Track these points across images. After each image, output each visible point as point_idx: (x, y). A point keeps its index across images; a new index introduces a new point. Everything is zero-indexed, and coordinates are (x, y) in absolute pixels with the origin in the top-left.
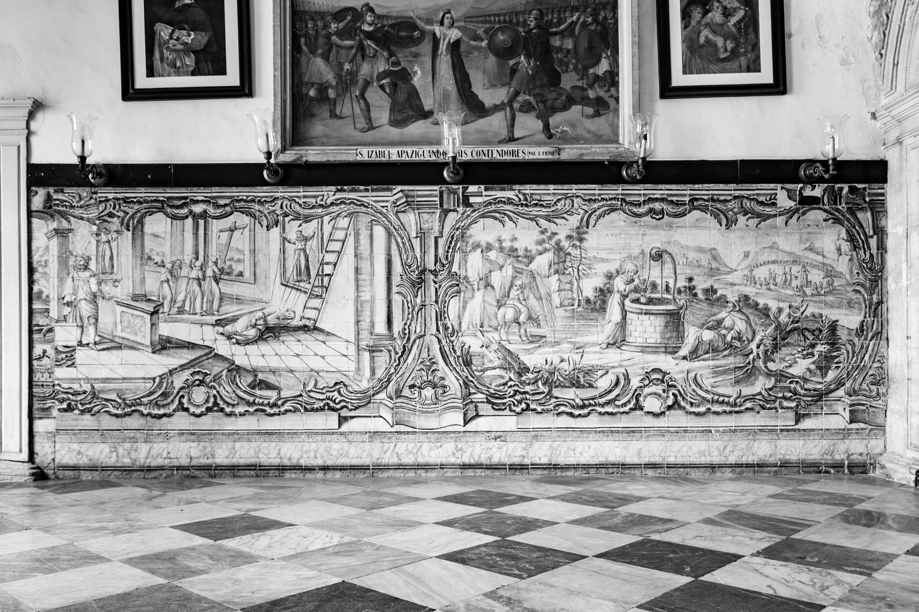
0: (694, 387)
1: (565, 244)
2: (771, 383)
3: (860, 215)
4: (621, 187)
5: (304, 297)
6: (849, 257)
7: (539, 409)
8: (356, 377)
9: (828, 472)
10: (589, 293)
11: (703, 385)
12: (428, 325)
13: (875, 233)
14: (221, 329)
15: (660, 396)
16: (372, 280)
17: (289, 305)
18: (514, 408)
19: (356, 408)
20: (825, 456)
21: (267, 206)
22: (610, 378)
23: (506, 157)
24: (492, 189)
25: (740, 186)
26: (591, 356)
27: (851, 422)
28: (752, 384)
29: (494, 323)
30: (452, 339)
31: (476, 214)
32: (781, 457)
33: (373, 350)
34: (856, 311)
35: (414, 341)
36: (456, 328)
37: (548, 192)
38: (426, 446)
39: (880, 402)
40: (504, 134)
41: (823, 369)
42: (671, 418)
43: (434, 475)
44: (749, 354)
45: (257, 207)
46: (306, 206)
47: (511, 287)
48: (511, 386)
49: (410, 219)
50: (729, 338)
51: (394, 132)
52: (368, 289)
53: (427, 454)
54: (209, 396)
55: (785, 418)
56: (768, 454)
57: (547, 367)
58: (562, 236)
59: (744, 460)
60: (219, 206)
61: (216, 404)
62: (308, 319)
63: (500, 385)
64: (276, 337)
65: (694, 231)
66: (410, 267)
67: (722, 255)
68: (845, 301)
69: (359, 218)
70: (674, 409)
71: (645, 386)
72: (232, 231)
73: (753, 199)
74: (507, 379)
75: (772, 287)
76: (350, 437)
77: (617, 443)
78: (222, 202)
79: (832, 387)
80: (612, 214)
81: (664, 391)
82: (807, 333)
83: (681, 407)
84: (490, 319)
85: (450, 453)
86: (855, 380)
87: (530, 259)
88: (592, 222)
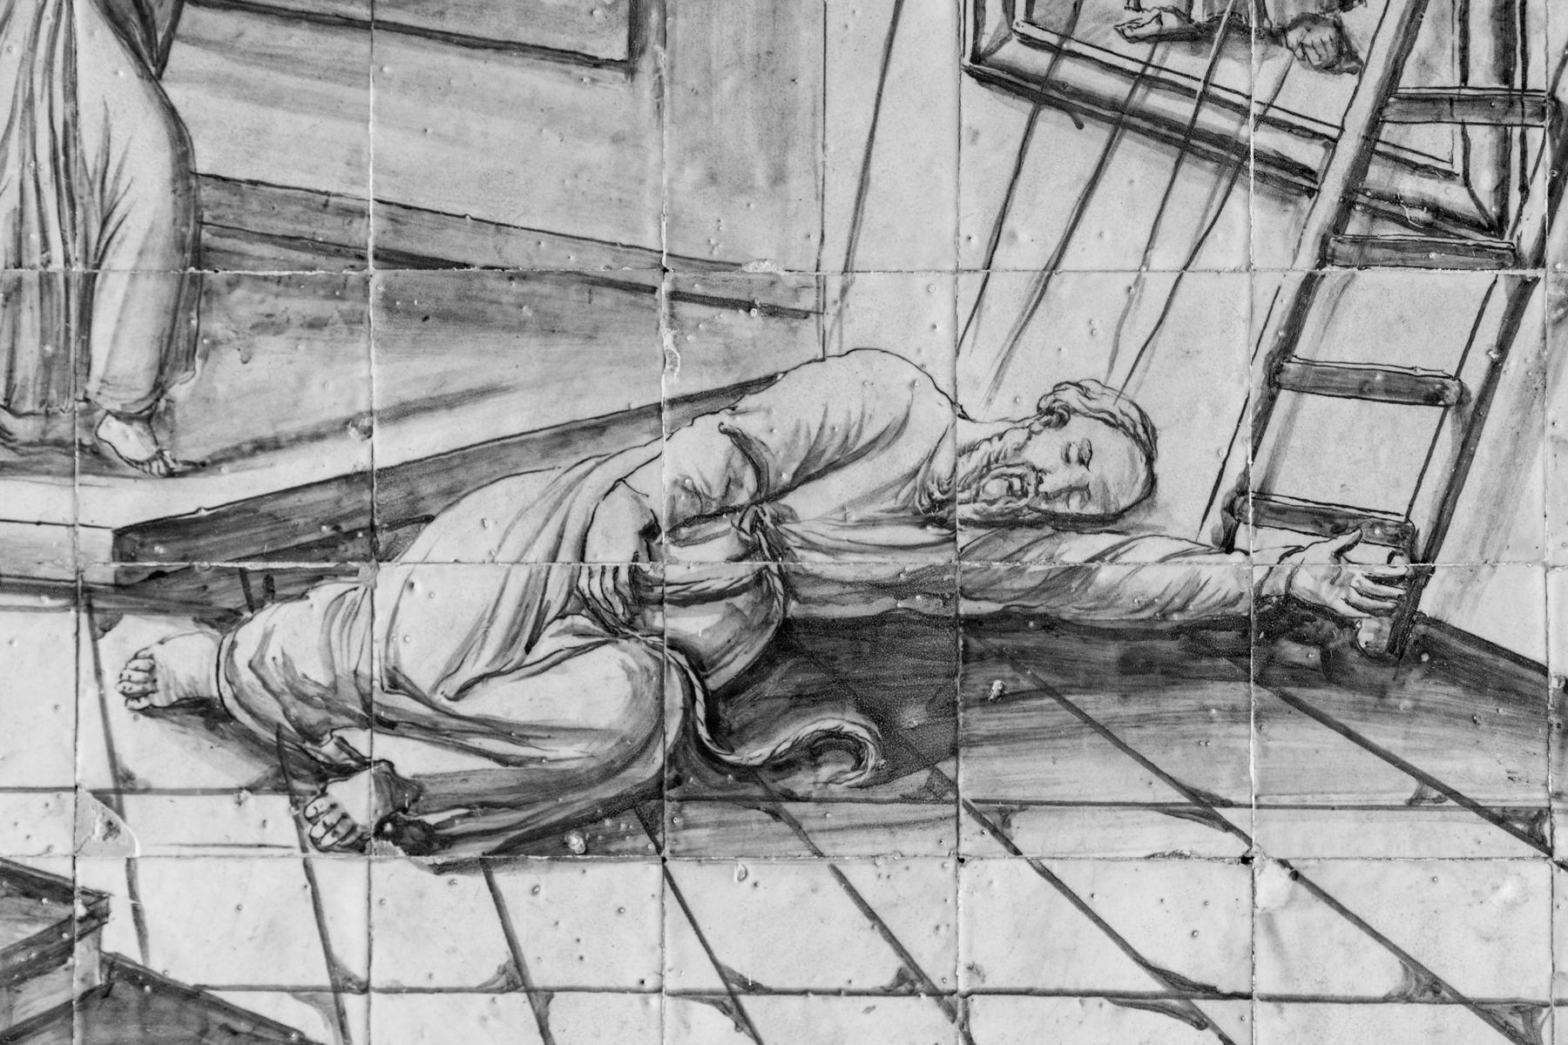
5: (1261, 241)
14: (187, 655)
17: (1071, 346)
62: (1326, 519)
64: (900, 754)
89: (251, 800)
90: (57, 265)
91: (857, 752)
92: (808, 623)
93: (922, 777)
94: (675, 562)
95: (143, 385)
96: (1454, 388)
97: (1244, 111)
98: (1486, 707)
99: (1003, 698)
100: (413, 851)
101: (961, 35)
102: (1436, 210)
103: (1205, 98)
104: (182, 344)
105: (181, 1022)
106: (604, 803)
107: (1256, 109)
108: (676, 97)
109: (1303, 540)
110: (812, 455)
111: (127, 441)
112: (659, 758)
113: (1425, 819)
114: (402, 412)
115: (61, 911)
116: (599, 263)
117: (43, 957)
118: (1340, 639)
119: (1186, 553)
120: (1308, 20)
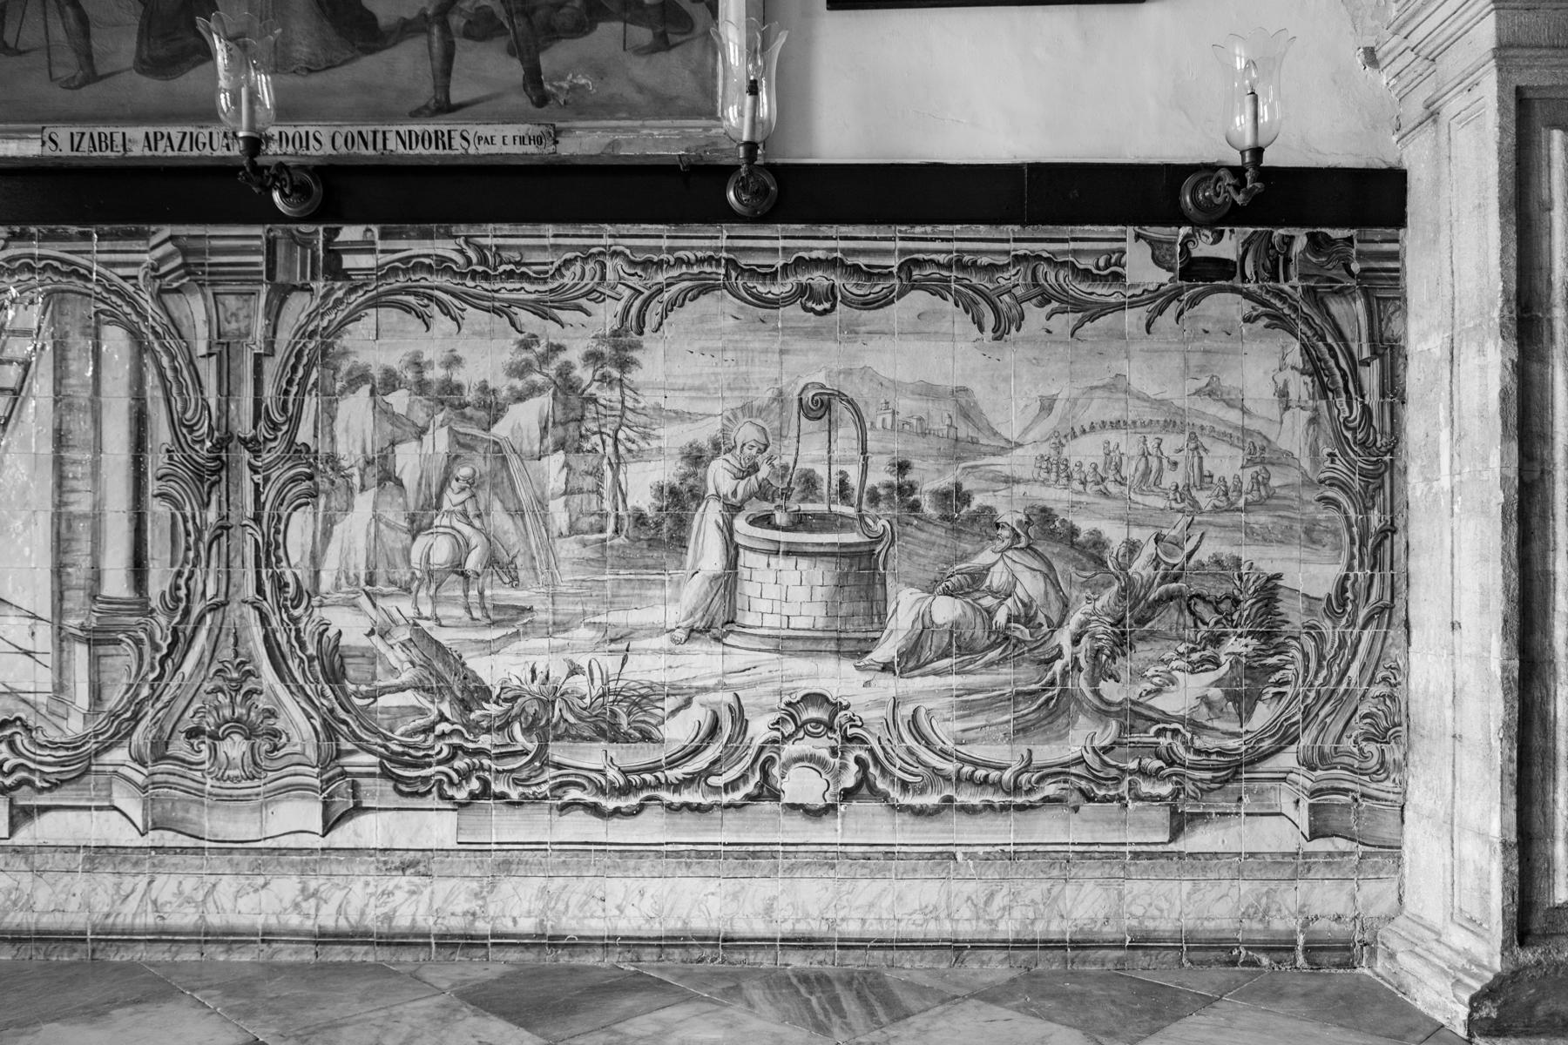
0: (910, 741)
1: (584, 374)
2: (1107, 733)
3: (1336, 307)
4: (725, 230)
6: (1308, 414)
7: (514, 794)
8: (55, 706)
9: (1255, 963)
10: (642, 498)
11: (933, 738)
12: (235, 577)
13: (1375, 353)
15: (822, 763)
16: (96, 466)
18: (450, 792)
19: (54, 786)
20: (1246, 923)
22: (697, 715)
23: (420, 150)
24: (398, 235)
25: (1029, 231)
26: (648, 661)
27: (1314, 834)
28: (1061, 737)
29: (402, 574)
30: (296, 613)
31: (357, 298)
32: (1134, 923)
33: (97, 639)
34: (1327, 551)
35: (201, 618)
36: (306, 584)
37: (542, 242)
38: (227, 885)
39: (1388, 784)
40: (426, 93)
41: (1242, 700)
42: (850, 821)
43: (246, 958)
44: (1053, 660)
47: (444, 484)
48: (443, 735)
49: (194, 309)
50: (1001, 618)
51: (150, 88)
53: (228, 905)
55: (1143, 822)
56: (1101, 916)
57: (535, 687)
58: (574, 354)
59: (1039, 930)
63: (414, 732)
65: (914, 345)
66: (191, 431)
67: (985, 407)
68: (1298, 527)
70: (860, 798)
71: (786, 739)
73: (1064, 264)
74: (433, 716)
75: (1113, 488)
76: (38, 860)
77: (712, 885)
79: (1266, 744)
80: (704, 300)
81: (834, 752)
82: (1200, 608)
83: (876, 794)
84: (391, 564)
85: (287, 903)
86: (1323, 728)
87: (494, 411)
88: (652, 319)
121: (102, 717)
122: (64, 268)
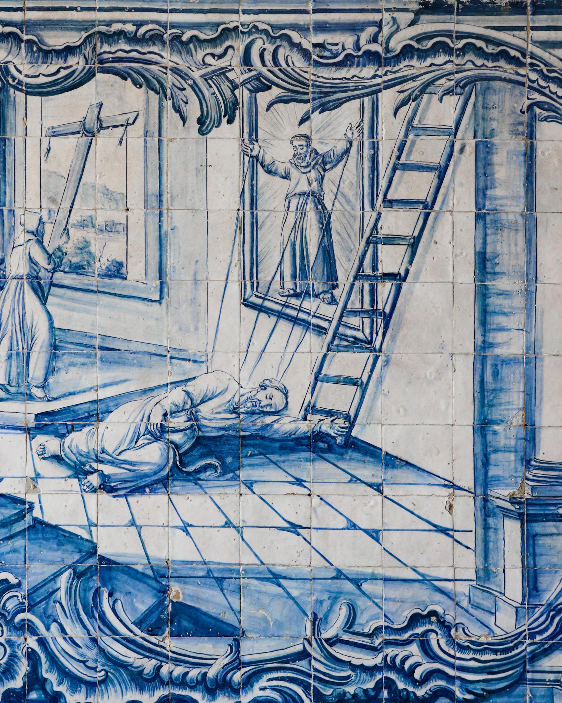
5: (314, 344)
8: (478, 597)
14: (52, 444)
16: (530, 295)
17: (268, 370)
21: (200, 54)
33: (531, 513)
45: (169, 58)
46: (322, 56)
52: (516, 321)
54: (13, 657)
60: (47, 54)
61: (35, 680)
62: (329, 413)
64: (226, 469)
69: (493, 99)
72: (90, 133)
78: (56, 40)
89: (69, 480)
90: (21, 350)
91: (215, 468)
92: (204, 437)
93: (231, 475)
94: (171, 422)
95: (42, 379)
96: (360, 381)
97: (309, 314)
98: (367, 458)
99: (251, 456)
100: (108, 492)
101: (241, 295)
102: (355, 338)
103: (300, 310)
104: (51, 369)
105: (52, 534)
106: (154, 481)
107: (312, 314)
108: (171, 309)
109: (324, 418)
110: (205, 396)
111: (38, 393)
112: (167, 470)
113: (352, 485)
114: (105, 386)
115: (22, 507)
116: (153, 350)
117: (18, 518)
118: (332, 442)
119: (295, 421)
120: (325, 292)
121: (538, 611)
122: (490, 49)
